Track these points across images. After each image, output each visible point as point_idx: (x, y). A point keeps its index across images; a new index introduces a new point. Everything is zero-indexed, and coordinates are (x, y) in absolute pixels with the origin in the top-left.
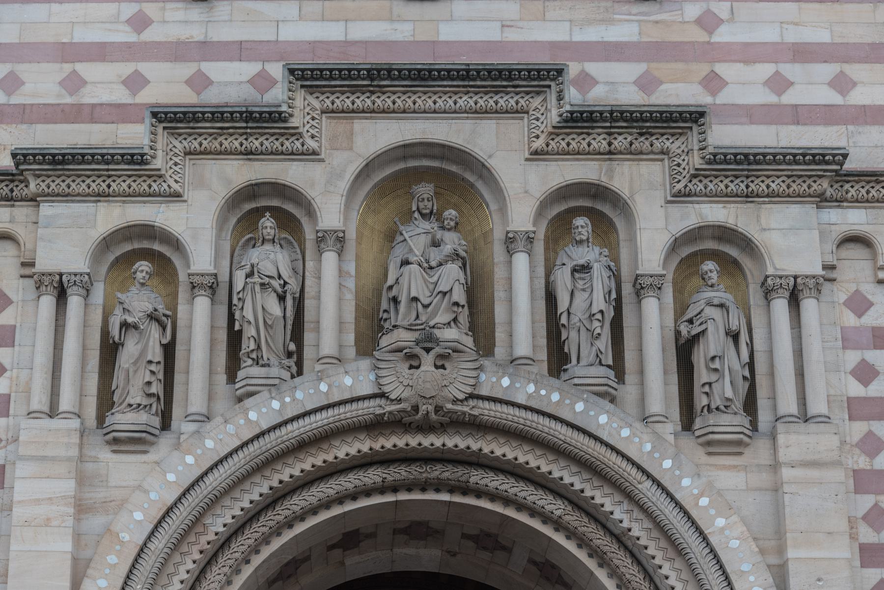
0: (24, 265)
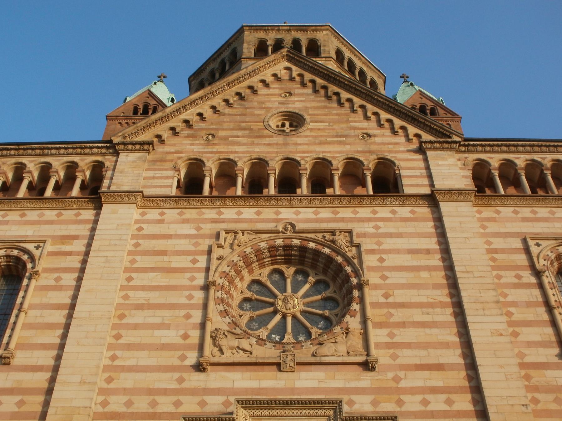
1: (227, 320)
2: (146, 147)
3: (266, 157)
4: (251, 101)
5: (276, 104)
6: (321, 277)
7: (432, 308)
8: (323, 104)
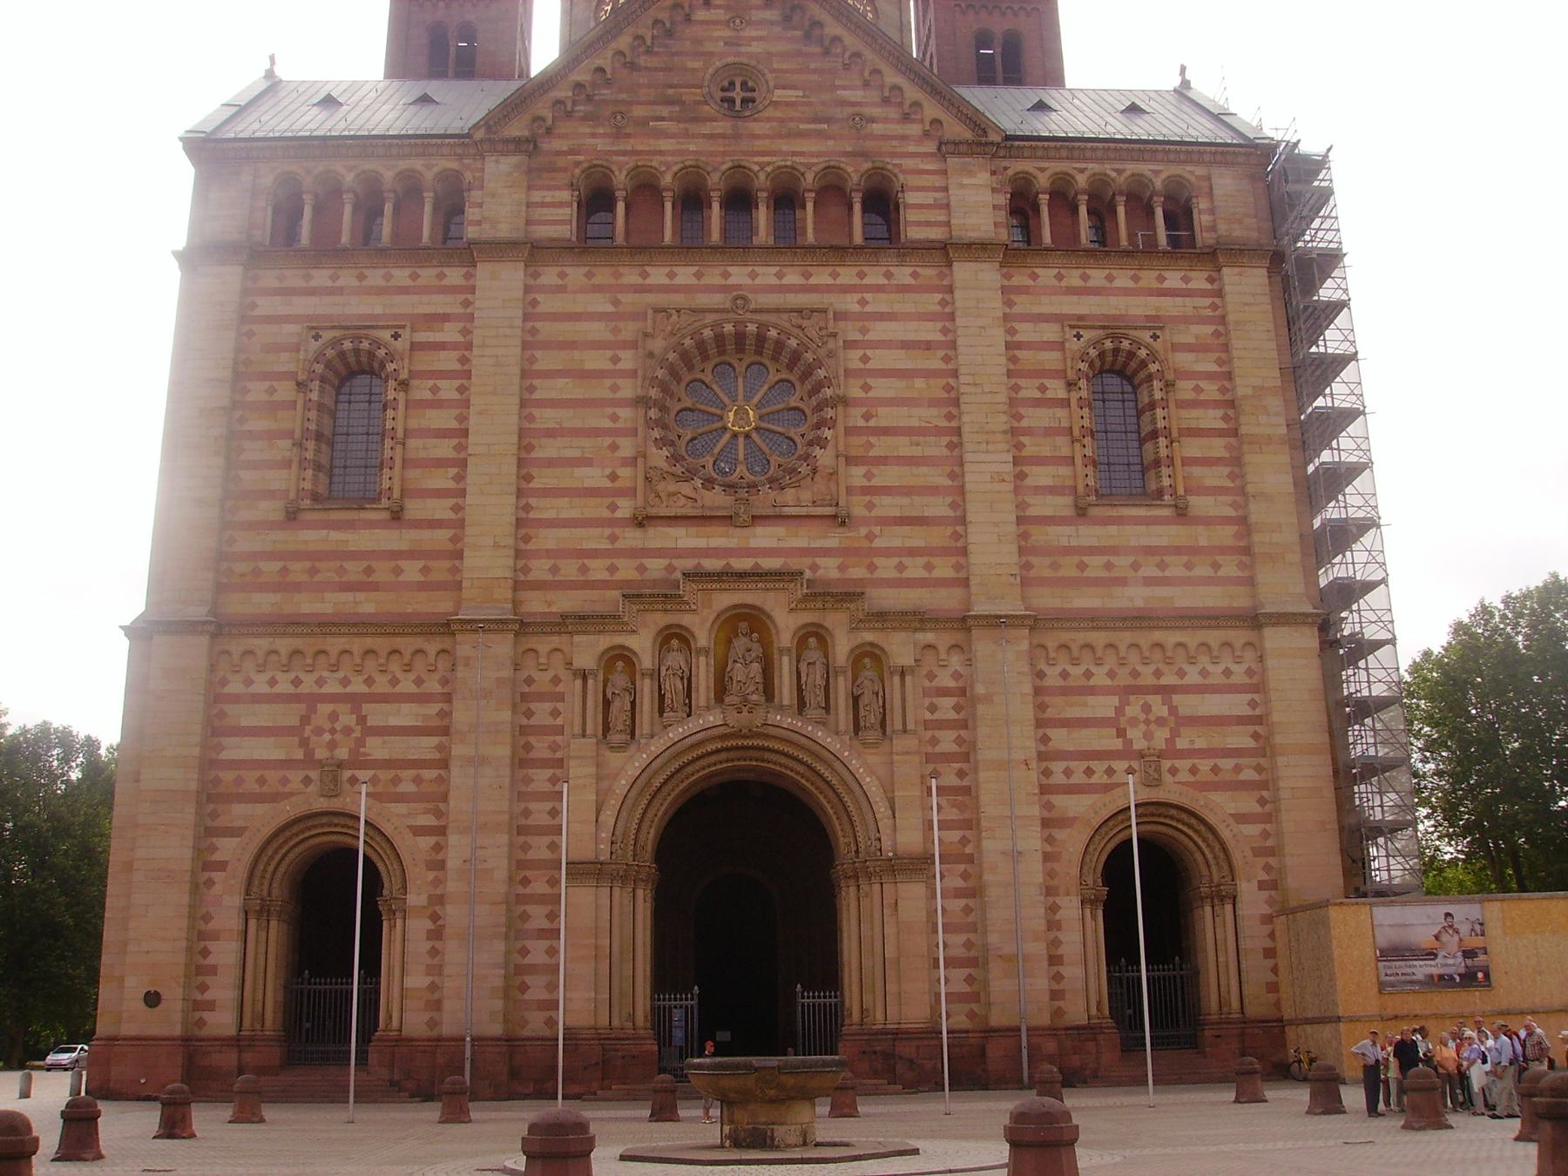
0: (567, 664)
1: (665, 452)
3: (707, 163)
6: (784, 376)
7: (924, 436)
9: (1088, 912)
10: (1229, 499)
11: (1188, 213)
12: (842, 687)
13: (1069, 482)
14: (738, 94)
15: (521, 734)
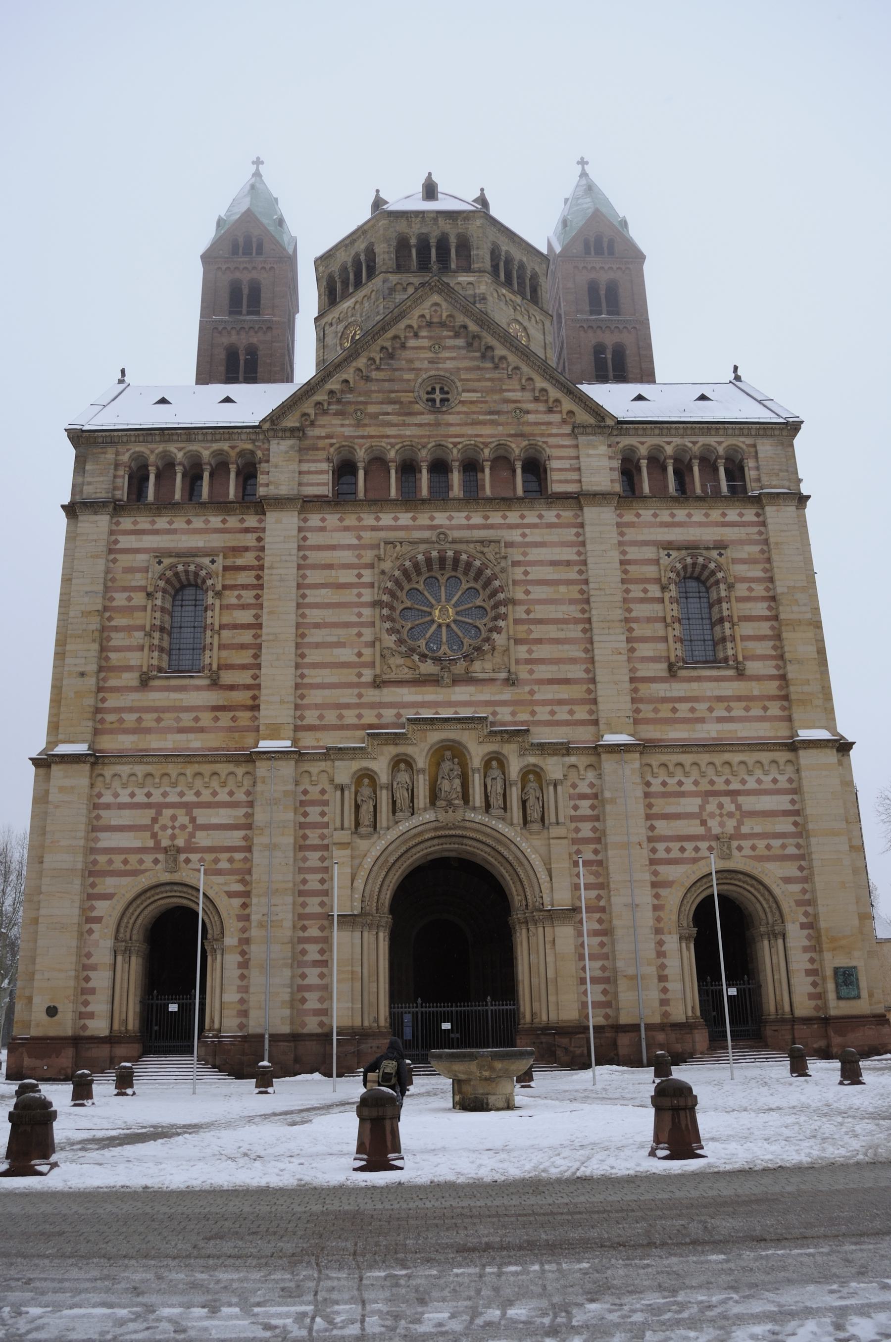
1: (394, 637)
2: (296, 434)
4: (399, 359)
5: (425, 364)
8: (476, 363)
9: (684, 945)
10: (774, 663)
11: (742, 469)
12: (515, 794)
13: (664, 654)
14: (438, 396)
15: (300, 828)
